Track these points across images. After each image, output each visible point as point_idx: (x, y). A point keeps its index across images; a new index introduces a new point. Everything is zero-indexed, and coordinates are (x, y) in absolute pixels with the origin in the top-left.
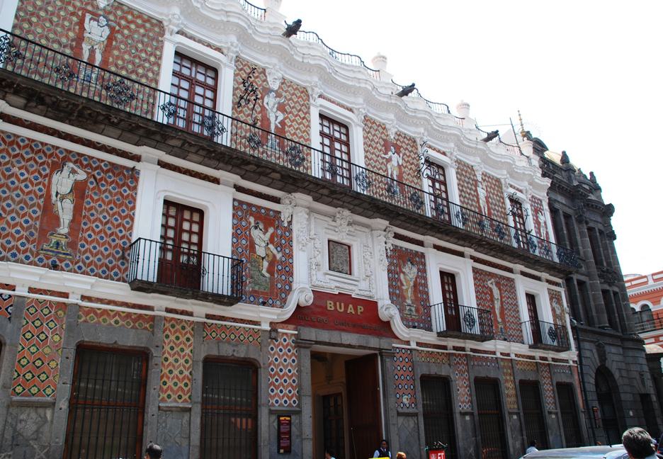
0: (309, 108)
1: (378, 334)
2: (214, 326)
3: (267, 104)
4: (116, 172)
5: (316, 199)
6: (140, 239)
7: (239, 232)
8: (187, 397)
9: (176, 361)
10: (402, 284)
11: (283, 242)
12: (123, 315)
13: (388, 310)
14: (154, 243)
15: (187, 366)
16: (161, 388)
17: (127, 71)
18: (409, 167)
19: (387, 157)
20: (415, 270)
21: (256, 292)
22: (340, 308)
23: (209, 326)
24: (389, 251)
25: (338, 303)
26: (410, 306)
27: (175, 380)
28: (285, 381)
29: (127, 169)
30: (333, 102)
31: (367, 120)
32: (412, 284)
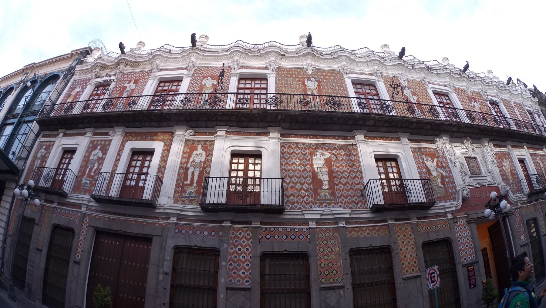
2: (422, 224)
6: (370, 180)
9: (407, 249)
15: (413, 251)
16: (402, 267)
27: (409, 261)
28: (467, 246)
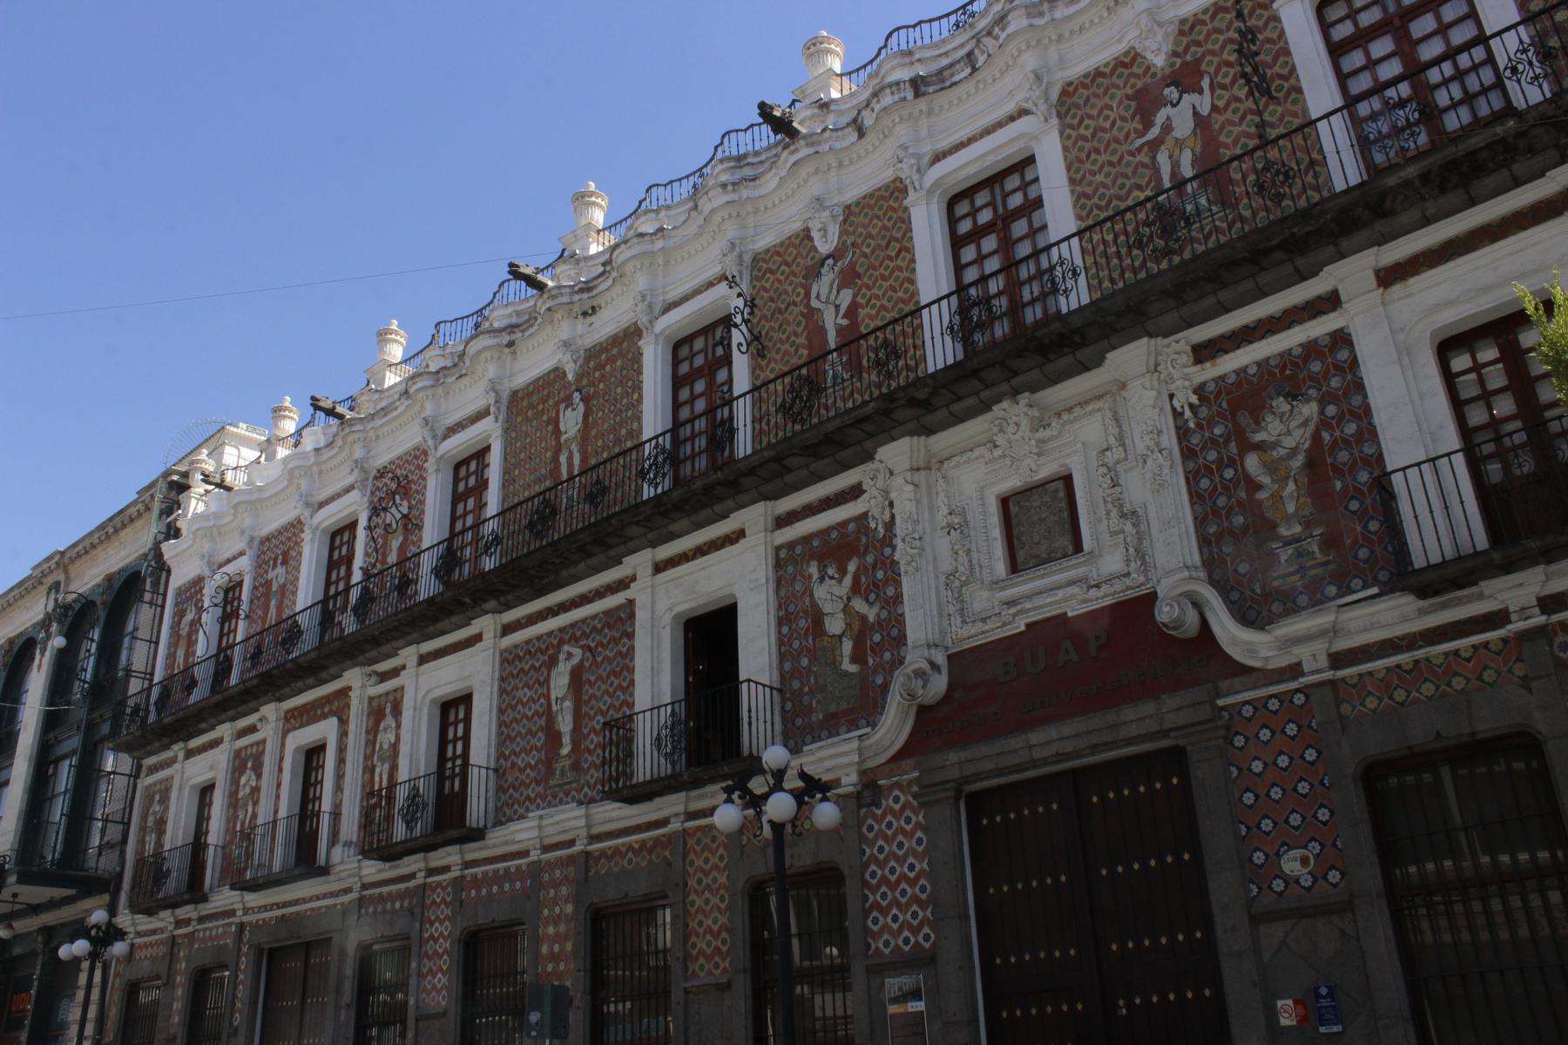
3: (818, 297)
9: (707, 901)
26: (1299, 540)
28: (903, 893)
29: (619, 608)
30: (971, 140)
32: (1298, 462)
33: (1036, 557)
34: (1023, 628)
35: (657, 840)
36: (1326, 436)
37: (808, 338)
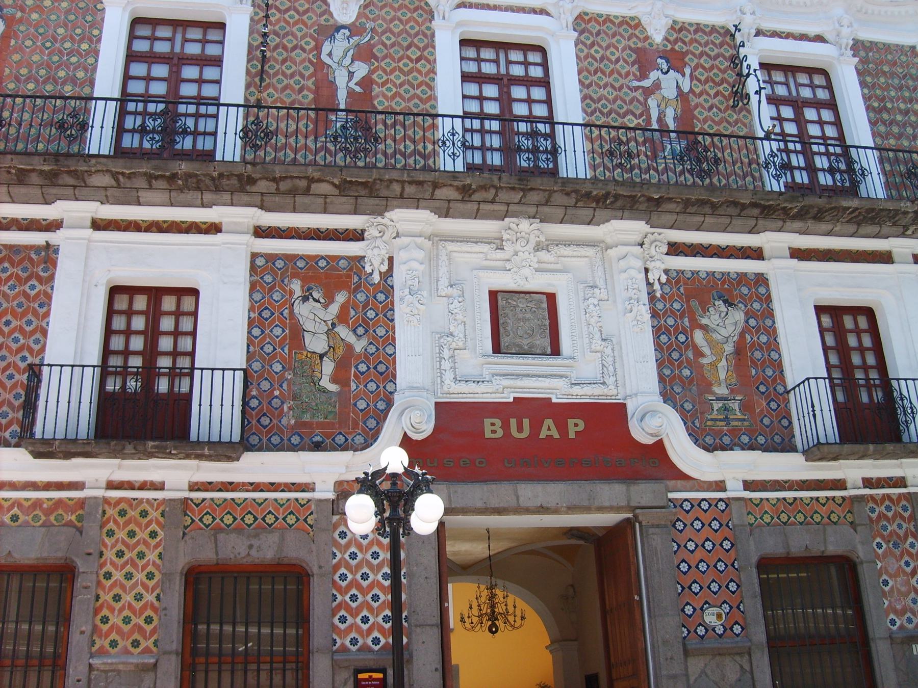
0: (433, 35)
1: (631, 476)
2: (207, 503)
3: (330, 55)
4: (17, 258)
5: (445, 213)
7: (266, 314)
8: (150, 643)
9: (129, 576)
10: (699, 354)
11: (371, 314)
12: (26, 504)
13: (656, 421)
14: (229, 374)
15: (151, 584)
16: (95, 629)
17: (37, 81)
18: (712, 92)
19: (646, 83)
20: (738, 316)
21: (305, 424)
22: (520, 429)
23: (197, 505)
24: (657, 286)
25: (513, 422)
26: (726, 399)
27: (126, 613)
29: (37, 249)
31: (582, 22)
32: (729, 348)
33: (518, 346)
34: (511, 400)
35: (59, 503)
36: (748, 337)
37: (316, 84)
